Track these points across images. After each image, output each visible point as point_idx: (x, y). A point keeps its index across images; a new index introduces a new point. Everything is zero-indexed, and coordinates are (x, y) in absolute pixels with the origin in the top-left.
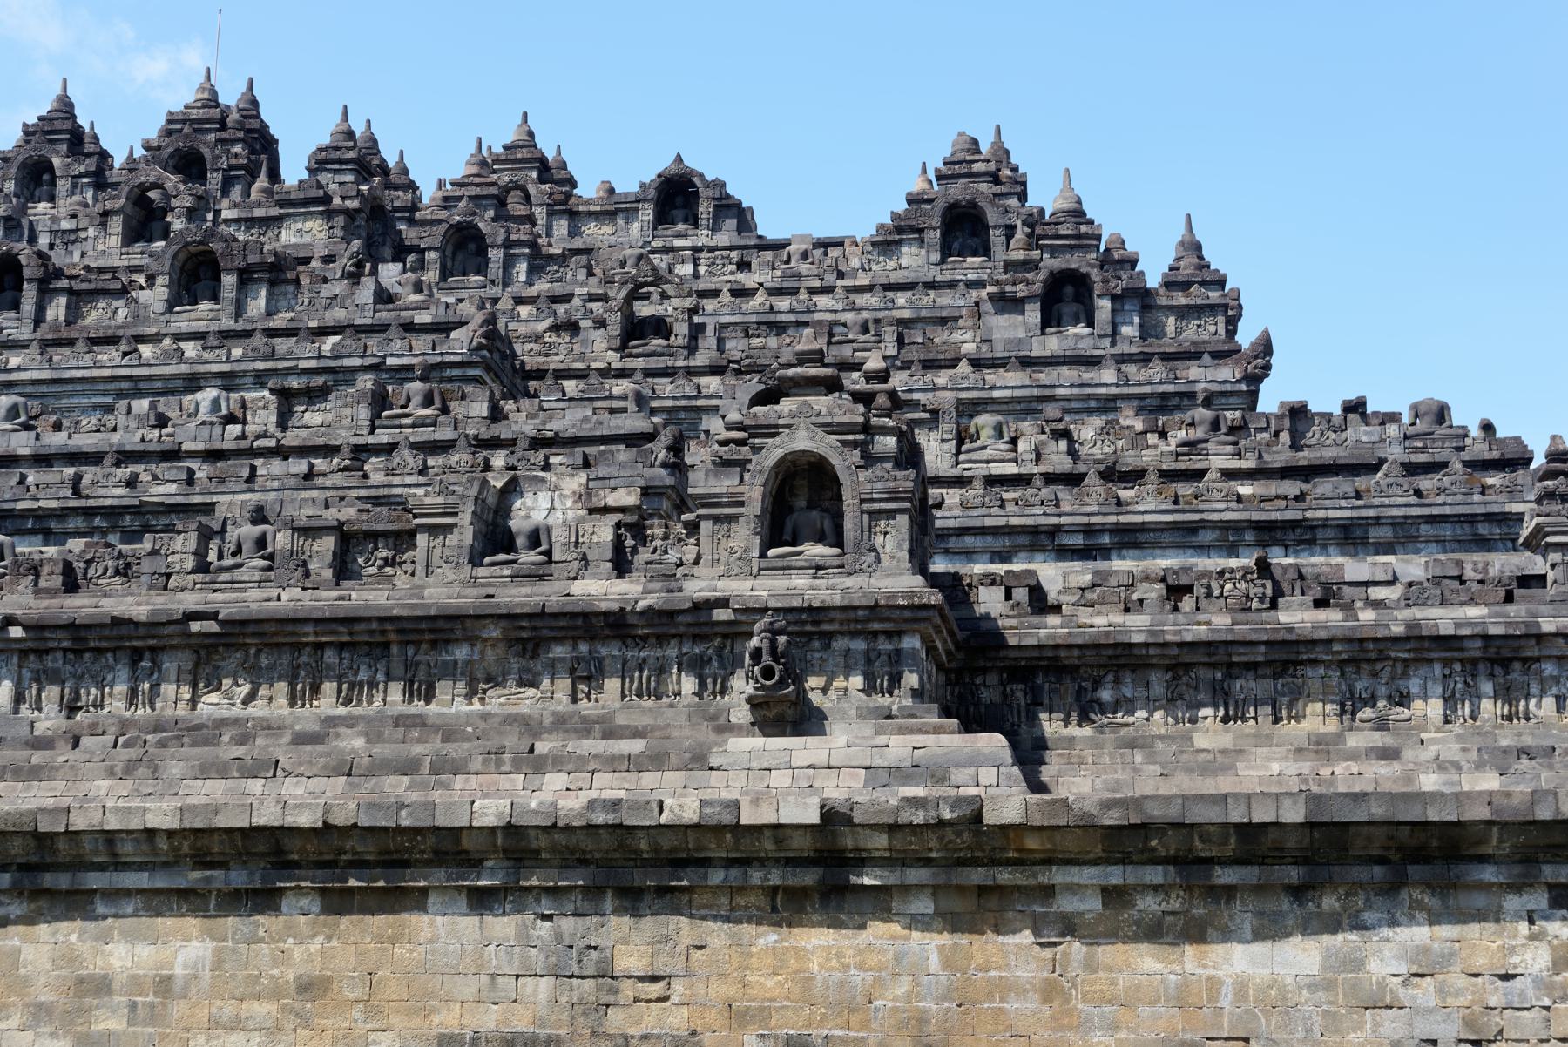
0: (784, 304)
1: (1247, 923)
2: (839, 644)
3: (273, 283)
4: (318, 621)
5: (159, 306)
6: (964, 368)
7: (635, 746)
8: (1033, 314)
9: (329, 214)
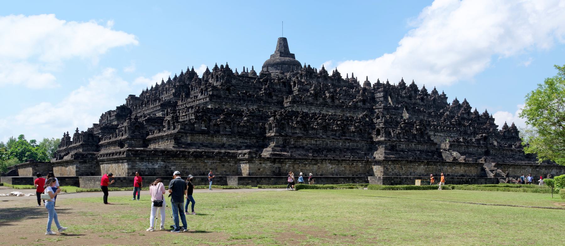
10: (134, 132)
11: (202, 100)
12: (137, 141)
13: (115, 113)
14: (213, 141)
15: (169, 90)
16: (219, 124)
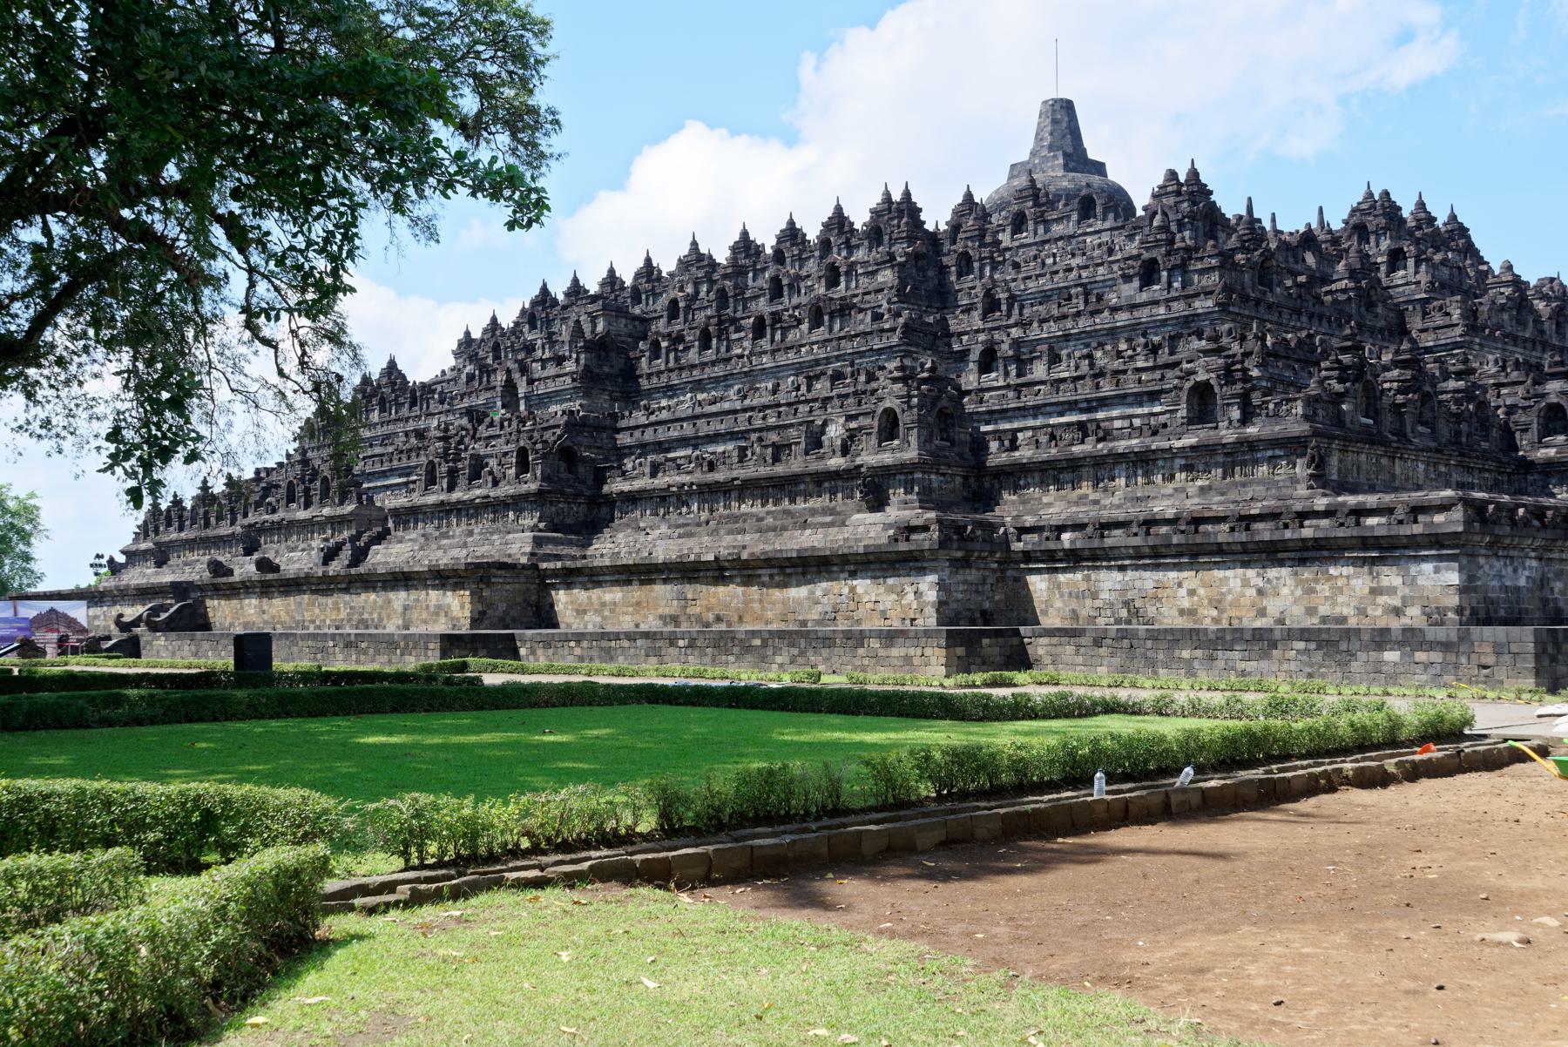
0: (1084, 274)
1: (794, 582)
3: (842, 316)
5: (806, 331)
6: (1106, 313)
8: (1136, 283)
9: (892, 267)
10: (929, 439)
11: (1162, 310)
14: (1393, 476)
15: (847, 273)
16: (1403, 405)
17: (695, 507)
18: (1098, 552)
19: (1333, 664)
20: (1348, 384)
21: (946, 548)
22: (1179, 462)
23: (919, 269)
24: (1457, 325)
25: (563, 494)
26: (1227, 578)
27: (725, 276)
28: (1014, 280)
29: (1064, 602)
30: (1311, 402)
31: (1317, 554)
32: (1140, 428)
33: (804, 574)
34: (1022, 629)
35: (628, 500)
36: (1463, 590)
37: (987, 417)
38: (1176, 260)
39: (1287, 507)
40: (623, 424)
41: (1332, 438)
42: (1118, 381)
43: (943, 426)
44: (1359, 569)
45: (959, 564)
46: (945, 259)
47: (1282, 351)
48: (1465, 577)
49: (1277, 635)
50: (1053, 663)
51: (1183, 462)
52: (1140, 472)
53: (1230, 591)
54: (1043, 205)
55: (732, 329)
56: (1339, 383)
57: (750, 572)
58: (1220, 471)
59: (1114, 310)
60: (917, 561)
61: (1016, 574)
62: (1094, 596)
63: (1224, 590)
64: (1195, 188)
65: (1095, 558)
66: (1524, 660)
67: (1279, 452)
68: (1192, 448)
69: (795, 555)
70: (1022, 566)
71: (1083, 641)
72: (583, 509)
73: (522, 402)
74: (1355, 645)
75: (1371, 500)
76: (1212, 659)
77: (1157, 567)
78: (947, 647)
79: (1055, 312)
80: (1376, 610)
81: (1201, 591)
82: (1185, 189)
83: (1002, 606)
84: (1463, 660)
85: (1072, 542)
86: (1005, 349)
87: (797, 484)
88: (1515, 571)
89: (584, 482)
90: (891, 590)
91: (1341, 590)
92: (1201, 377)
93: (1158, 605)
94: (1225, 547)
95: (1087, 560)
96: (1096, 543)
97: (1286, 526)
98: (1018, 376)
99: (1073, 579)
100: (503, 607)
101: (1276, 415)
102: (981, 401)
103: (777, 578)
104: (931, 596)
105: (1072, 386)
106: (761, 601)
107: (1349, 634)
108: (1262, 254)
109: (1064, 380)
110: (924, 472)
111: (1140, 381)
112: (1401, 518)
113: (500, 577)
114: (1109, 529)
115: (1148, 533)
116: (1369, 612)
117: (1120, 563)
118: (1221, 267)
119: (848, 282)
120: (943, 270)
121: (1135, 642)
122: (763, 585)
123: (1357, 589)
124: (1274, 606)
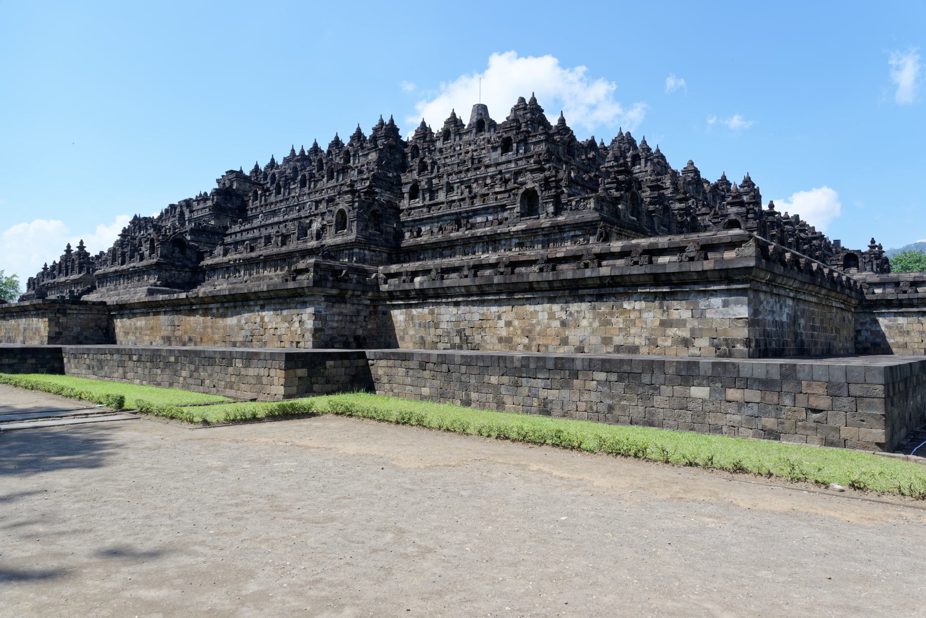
1: (230, 314)
2: (345, 252)
3: (344, 173)
4: (276, 255)
7: (271, 277)
9: (376, 151)
10: (366, 228)
12: (374, 251)
13: (209, 203)
15: (354, 156)
17: (242, 273)
18: (440, 291)
19: (635, 397)
20: (622, 192)
21: (320, 286)
22: (515, 241)
23: (391, 154)
24: (669, 188)
25: (173, 265)
26: (536, 312)
27: (298, 161)
28: (439, 159)
29: (415, 330)
30: (600, 200)
31: (613, 290)
32: (492, 222)
33: (235, 307)
34: (367, 351)
35: (212, 270)
36: (752, 322)
37: (412, 224)
38: (521, 137)
39: (588, 250)
40: (229, 232)
41: (613, 224)
42: (484, 200)
43: (376, 222)
44: (650, 304)
45: (334, 300)
46: (406, 150)
47: (580, 181)
48: (752, 311)
49: (578, 365)
50: (389, 382)
51: (517, 241)
52: (490, 248)
53: (538, 323)
54: (459, 126)
55: (292, 183)
56: (616, 191)
57: (206, 306)
58: (540, 246)
59: (487, 167)
60: (301, 296)
61: (384, 309)
62: (437, 326)
63: (534, 322)
64: (534, 107)
65: (437, 296)
66: (870, 406)
67: (578, 233)
68: (523, 231)
69: (227, 293)
70: (388, 303)
71: (413, 364)
72: (188, 275)
73: (187, 222)
74: (659, 378)
75: (662, 241)
76: (517, 385)
77: (482, 303)
78: (286, 369)
79: (456, 170)
80: (666, 341)
81: (516, 323)
82: (529, 106)
83: (374, 333)
84: (787, 401)
85: (421, 283)
86: (423, 184)
87: (292, 258)
88: (781, 308)
89: (190, 259)
90: (285, 320)
91: (634, 323)
92: (530, 185)
93: (483, 334)
94: (535, 286)
95: (432, 297)
96: (437, 284)
97: (586, 266)
98: (430, 200)
99: (421, 313)
100: (77, 329)
101: (577, 209)
102: (409, 215)
103: (221, 311)
104: (310, 324)
105: (458, 203)
106: (212, 327)
107: (651, 366)
108: (569, 137)
109: (454, 201)
110: (360, 249)
111: (496, 199)
112: (692, 255)
113: (76, 310)
114: (448, 273)
115: (475, 275)
116: (660, 343)
117: (455, 300)
118: (546, 140)
119: (354, 160)
120: (405, 155)
121: (452, 367)
122: (213, 316)
123: (649, 321)
124: (574, 336)
